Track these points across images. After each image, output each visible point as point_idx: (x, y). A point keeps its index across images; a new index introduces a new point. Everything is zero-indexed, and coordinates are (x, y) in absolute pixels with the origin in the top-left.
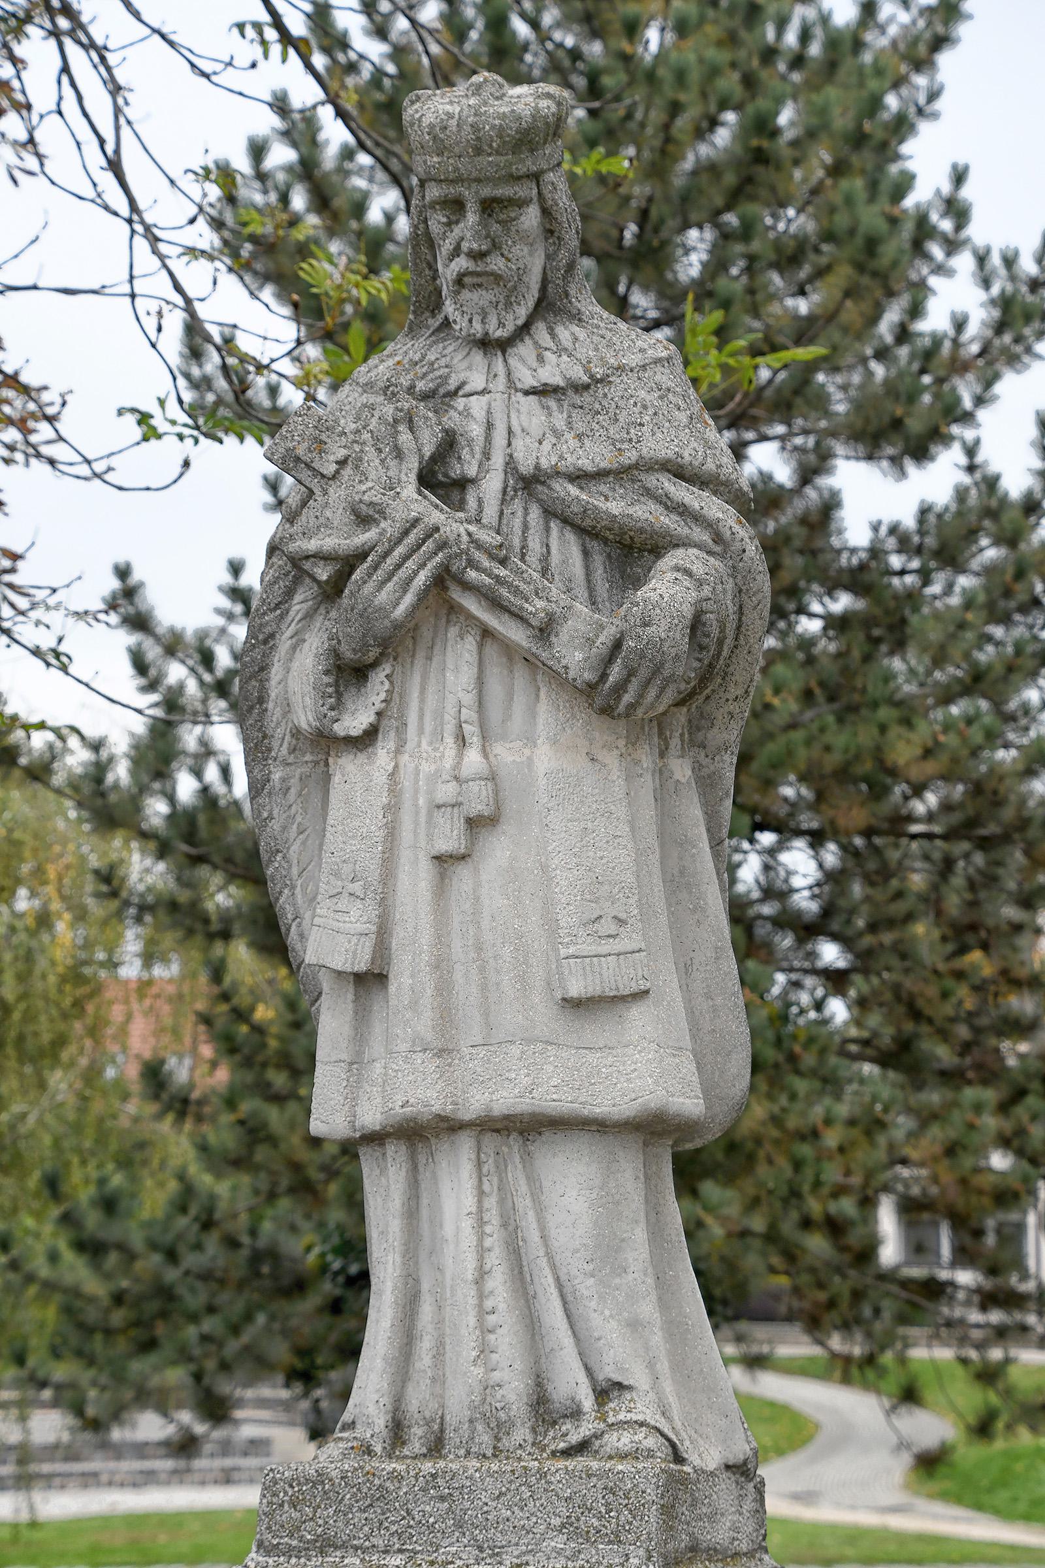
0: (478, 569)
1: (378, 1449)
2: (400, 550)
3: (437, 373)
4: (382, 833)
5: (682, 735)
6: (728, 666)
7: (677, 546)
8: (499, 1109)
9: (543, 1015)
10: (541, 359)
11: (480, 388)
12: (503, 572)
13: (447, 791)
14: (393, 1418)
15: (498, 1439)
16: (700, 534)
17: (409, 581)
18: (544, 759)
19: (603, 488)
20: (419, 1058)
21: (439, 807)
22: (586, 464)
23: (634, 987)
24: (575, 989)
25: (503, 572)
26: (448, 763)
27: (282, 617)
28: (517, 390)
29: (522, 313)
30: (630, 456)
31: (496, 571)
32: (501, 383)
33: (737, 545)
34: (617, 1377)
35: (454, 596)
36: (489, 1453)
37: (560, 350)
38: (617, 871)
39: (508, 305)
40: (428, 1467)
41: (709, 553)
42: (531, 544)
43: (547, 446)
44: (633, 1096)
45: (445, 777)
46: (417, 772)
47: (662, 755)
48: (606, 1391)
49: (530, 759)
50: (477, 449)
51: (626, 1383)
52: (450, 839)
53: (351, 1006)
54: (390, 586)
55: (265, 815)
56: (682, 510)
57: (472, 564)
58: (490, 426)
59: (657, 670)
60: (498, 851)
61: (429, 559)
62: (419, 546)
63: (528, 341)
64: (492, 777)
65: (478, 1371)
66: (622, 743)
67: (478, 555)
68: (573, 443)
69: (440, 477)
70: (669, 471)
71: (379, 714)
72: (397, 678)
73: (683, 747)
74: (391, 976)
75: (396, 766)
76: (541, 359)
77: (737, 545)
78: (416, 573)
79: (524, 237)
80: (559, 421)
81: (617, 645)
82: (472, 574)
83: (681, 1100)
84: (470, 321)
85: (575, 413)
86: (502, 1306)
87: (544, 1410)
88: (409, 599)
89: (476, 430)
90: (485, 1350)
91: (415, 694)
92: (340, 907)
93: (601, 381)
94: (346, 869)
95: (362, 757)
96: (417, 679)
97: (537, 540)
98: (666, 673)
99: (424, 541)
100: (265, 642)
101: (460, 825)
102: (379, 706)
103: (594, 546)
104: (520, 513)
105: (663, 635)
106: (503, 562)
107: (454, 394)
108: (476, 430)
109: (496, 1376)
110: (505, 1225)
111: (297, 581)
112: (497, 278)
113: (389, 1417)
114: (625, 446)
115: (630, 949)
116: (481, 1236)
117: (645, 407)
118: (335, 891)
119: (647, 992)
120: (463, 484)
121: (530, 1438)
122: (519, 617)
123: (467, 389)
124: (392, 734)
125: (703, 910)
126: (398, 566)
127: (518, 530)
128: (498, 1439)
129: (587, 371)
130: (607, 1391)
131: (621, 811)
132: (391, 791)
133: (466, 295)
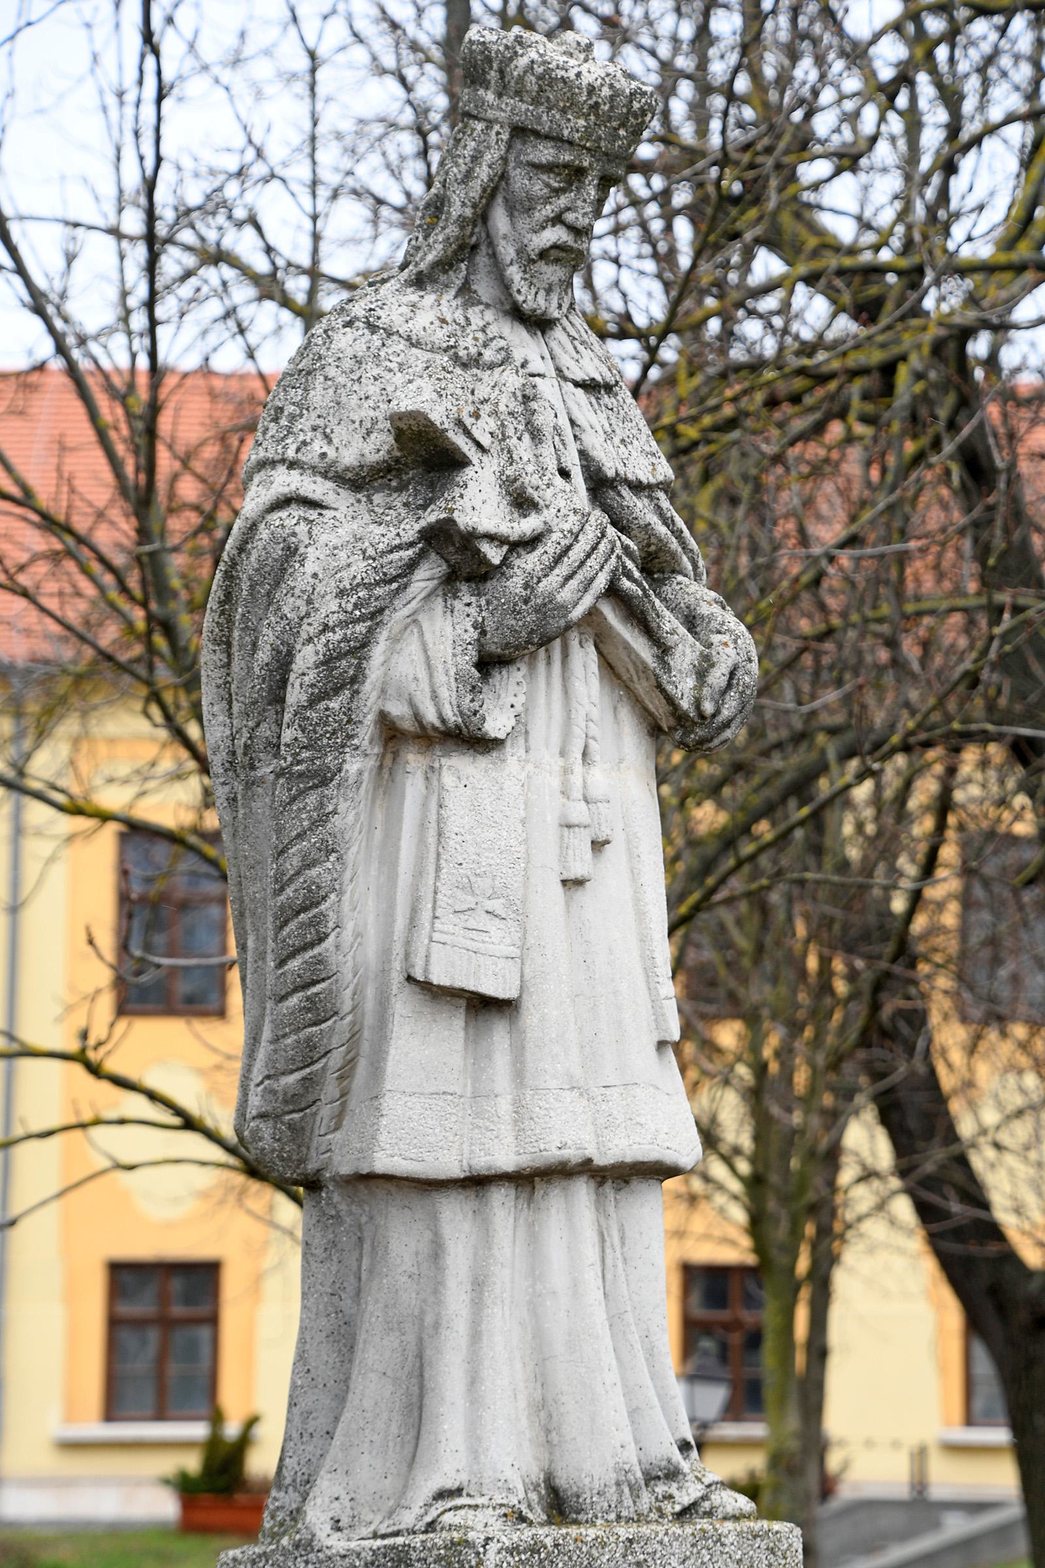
0: (630, 577)
17: (592, 580)
20: (568, 1096)
21: (569, 826)
27: (397, 591)
28: (566, 379)
53: (462, 1034)
54: (573, 584)
55: (331, 808)
74: (527, 1004)
92: (472, 924)
94: (479, 883)
95: (483, 762)
100: (373, 615)
102: (519, 708)
111: (422, 555)
118: (465, 907)
133: (542, 266)
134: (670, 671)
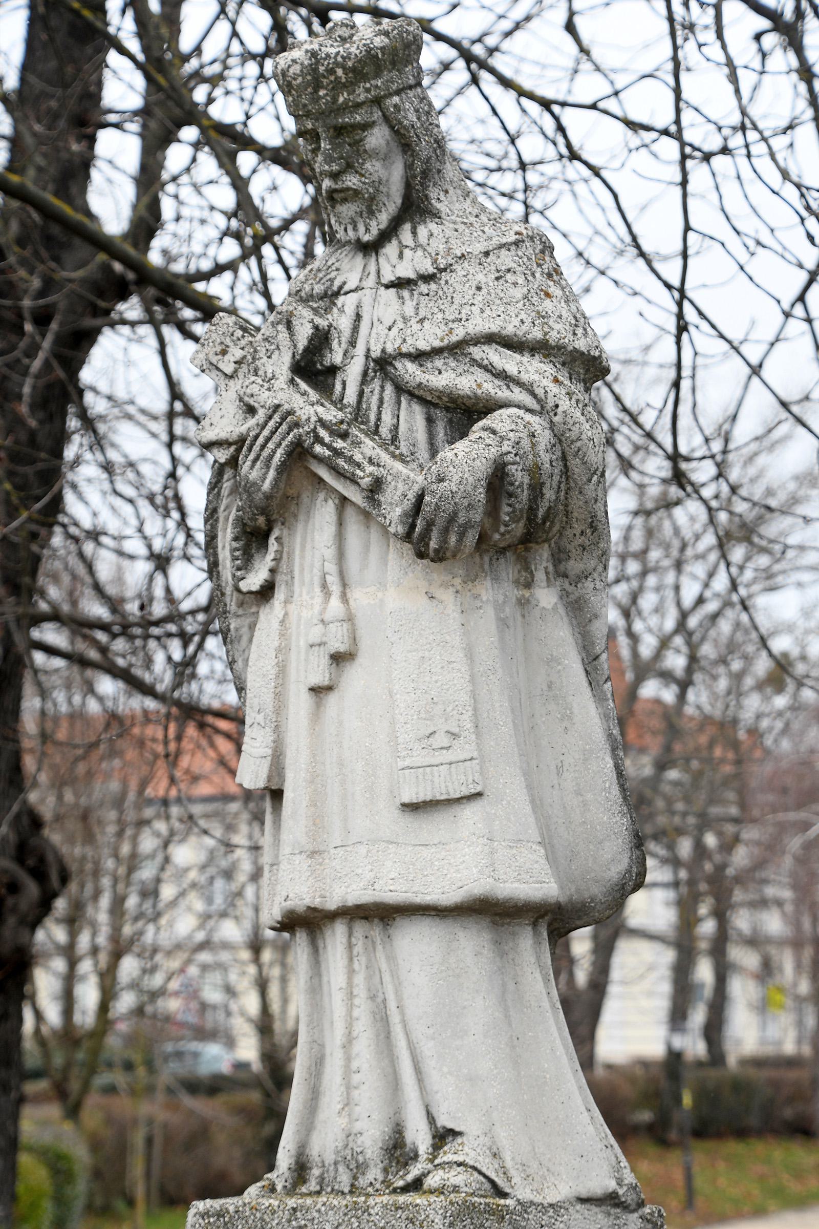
0: (323, 443)
1: (279, 1188)
2: (266, 432)
3: (328, 277)
4: (273, 671)
5: (546, 568)
6: (566, 506)
7: (501, 407)
8: (351, 901)
9: (390, 820)
10: (401, 256)
11: (353, 287)
12: (339, 444)
13: (316, 634)
14: (297, 1163)
15: (355, 1178)
16: (518, 395)
17: (271, 457)
18: (393, 600)
19: (439, 363)
20: (297, 859)
21: (311, 646)
22: (423, 346)
23: (465, 792)
24: (408, 797)
25: (339, 444)
26: (317, 609)
29: (383, 219)
30: (459, 333)
31: (335, 445)
32: (371, 281)
33: (551, 403)
34: (450, 1125)
35: (313, 468)
36: (346, 1190)
37: (417, 246)
38: (451, 691)
39: (371, 213)
40: (292, 1202)
41: (529, 410)
42: (384, 416)
43: (395, 330)
44: (460, 884)
45: (315, 621)
46: (299, 618)
47: (528, 585)
48: (443, 1137)
49: (382, 601)
50: (344, 340)
51: (457, 1129)
52: (319, 674)
56: (502, 376)
57: (319, 440)
58: (358, 317)
59: (452, 519)
60: (355, 678)
61: (283, 439)
62: (277, 429)
63: (394, 242)
64: (350, 618)
65: (343, 1122)
66: (457, 581)
67: (323, 433)
68: (416, 327)
69: (319, 366)
70: (498, 343)
71: (272, 571)
72: (285, 540)
73: (548, 579)
75: (286, 614)
76: (401, 256)
77: (551, 403)
78: (274, 452)
79: (374, 154)
80: (409, 309)
81: (420, 498)
82: (318, 449)
83: (516, 885)
84: (346, 230)
85: (424, 300)
86: (365, 1067)
87: (397, 1151)
88: (272, 474)
89: (344, 323)
90: (348, 1103)
91: (297, 552)
93: (445, 270)
96: (298, 539)
97: (389, 413)
98: (461, 520)
99: (281, 424)
101: (325, 661)
103: (438, 413)
104: (377, 392)
105: (454, 489)
106: (344, 436)
107: (337, 294)
108: (344, 323)
109: (358, 1126)
110: (373, 998)
112: (356, 193)
113: (292, 1161)
114: (455, 325)
115: (462, 758)
116: (350, 1007)
117: (479, 288)
119: (479, 795)
120: (333, 370)
121: (380, 1177)
122: (353, 480)
123: (346, 288)
124: (283, 587)
125: (570, 718)
126: (263, 447)
127: (374, 407)
128: (355, 1178)
129: (435, 261)
130: (443, 1137)
131: (456, 640)
132: (282, 635)
134: (379, 505)
